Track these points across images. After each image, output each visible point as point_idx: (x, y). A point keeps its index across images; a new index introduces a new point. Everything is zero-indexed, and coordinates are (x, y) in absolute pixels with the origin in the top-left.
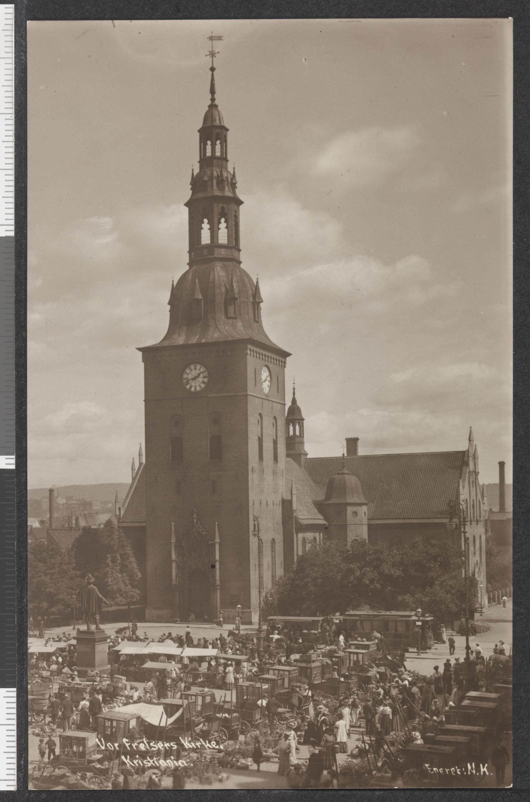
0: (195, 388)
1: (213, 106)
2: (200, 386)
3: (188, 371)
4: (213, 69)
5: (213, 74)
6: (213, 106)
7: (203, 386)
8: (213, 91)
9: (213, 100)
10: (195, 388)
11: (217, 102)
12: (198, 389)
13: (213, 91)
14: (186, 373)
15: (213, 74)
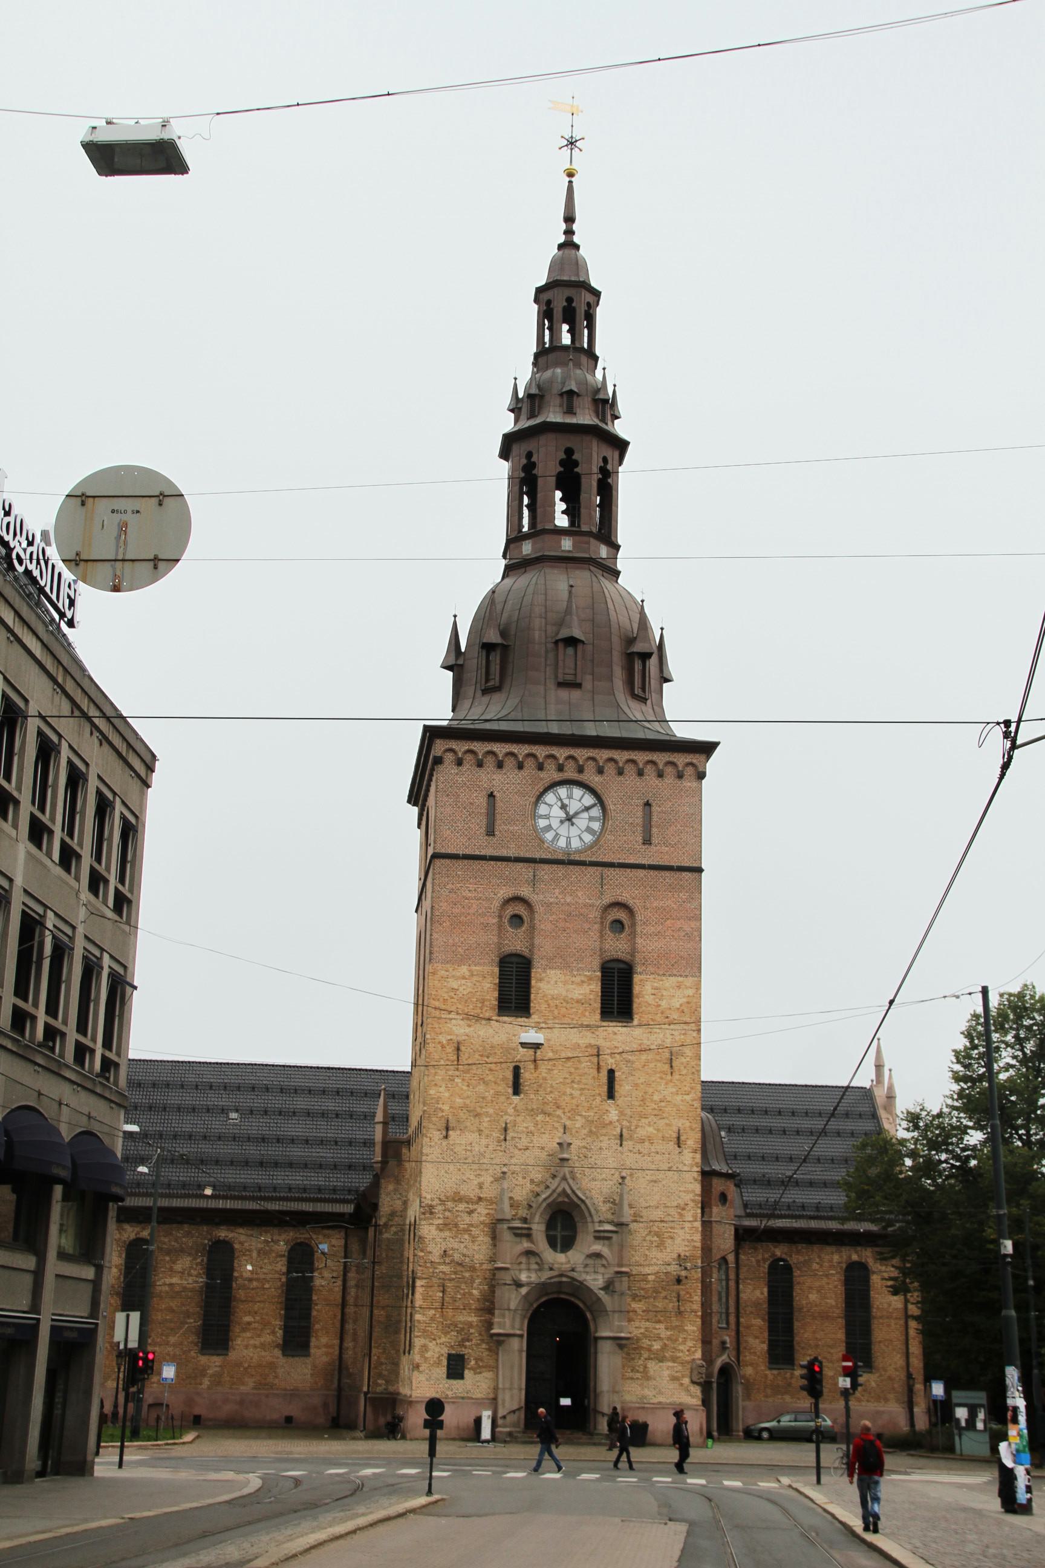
0: (569, 843)
1: (569, 245)
2: (581, 839)
3: (550, 797)
4: (571, 175)
5: (570, 182)
6: (569, 245)
7: (588, 838)
8: (569, 219)
9: (569, 232)
10: (569, 843)
11: (576, 239)
12: (576, 844)
13: (569, 219)
14: (546, 804)
15: (570, 182)
